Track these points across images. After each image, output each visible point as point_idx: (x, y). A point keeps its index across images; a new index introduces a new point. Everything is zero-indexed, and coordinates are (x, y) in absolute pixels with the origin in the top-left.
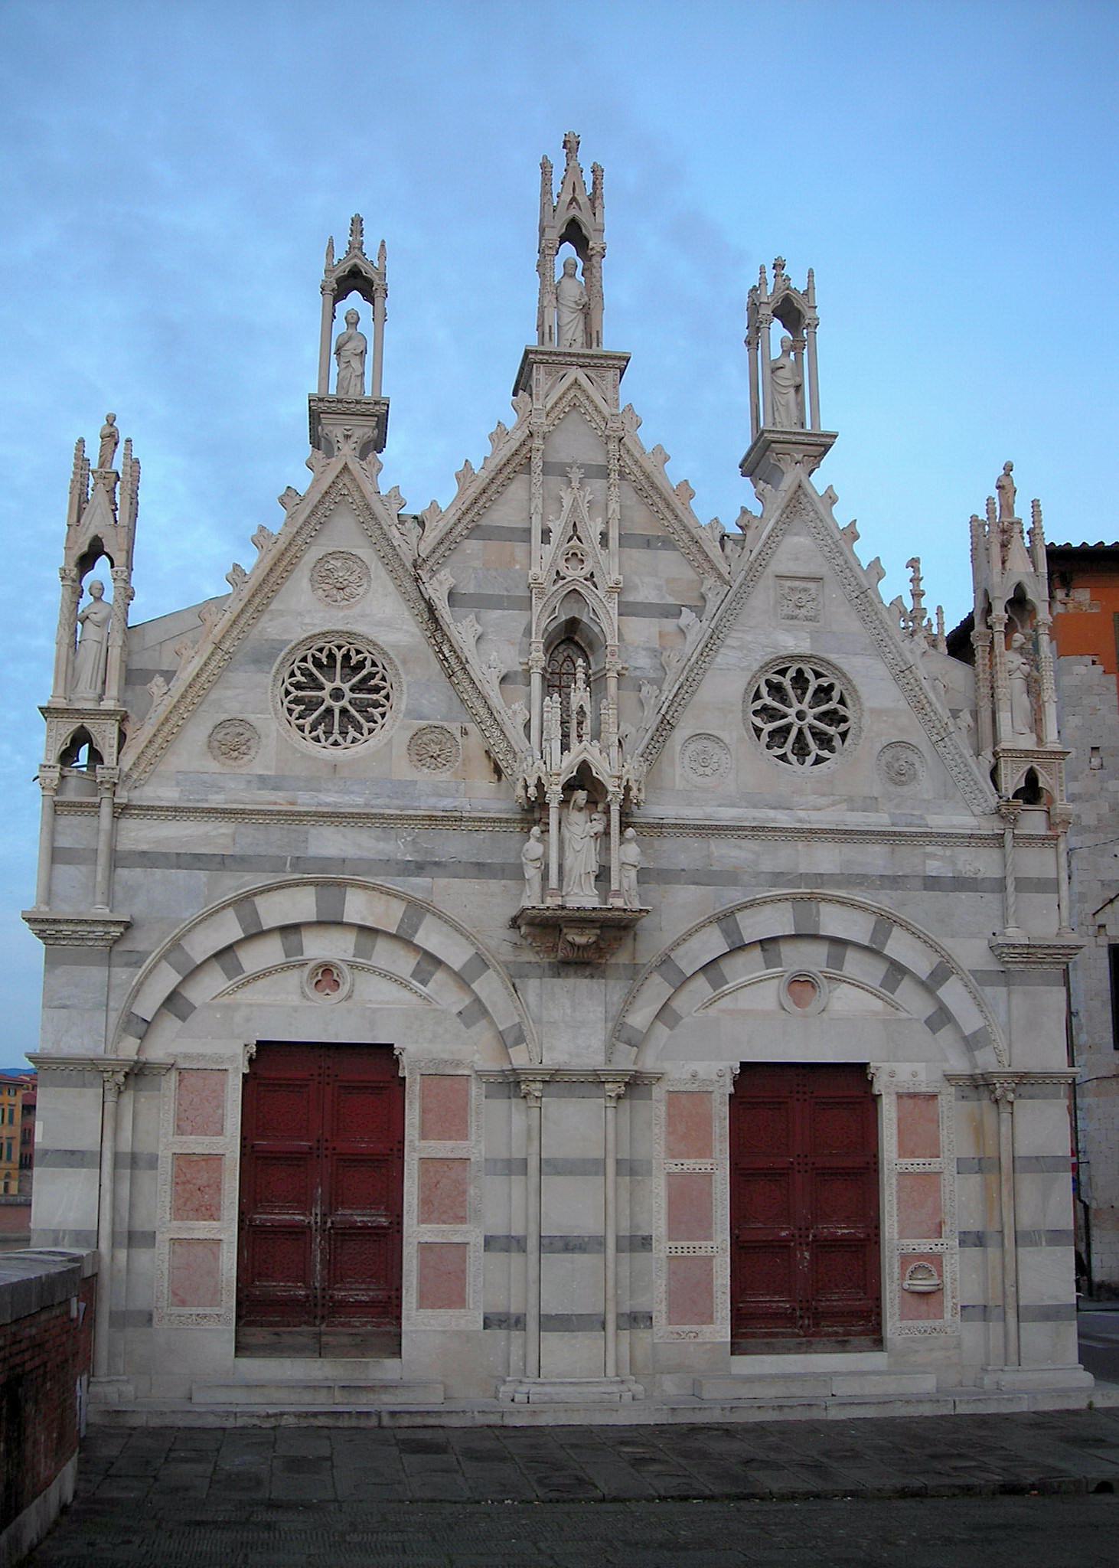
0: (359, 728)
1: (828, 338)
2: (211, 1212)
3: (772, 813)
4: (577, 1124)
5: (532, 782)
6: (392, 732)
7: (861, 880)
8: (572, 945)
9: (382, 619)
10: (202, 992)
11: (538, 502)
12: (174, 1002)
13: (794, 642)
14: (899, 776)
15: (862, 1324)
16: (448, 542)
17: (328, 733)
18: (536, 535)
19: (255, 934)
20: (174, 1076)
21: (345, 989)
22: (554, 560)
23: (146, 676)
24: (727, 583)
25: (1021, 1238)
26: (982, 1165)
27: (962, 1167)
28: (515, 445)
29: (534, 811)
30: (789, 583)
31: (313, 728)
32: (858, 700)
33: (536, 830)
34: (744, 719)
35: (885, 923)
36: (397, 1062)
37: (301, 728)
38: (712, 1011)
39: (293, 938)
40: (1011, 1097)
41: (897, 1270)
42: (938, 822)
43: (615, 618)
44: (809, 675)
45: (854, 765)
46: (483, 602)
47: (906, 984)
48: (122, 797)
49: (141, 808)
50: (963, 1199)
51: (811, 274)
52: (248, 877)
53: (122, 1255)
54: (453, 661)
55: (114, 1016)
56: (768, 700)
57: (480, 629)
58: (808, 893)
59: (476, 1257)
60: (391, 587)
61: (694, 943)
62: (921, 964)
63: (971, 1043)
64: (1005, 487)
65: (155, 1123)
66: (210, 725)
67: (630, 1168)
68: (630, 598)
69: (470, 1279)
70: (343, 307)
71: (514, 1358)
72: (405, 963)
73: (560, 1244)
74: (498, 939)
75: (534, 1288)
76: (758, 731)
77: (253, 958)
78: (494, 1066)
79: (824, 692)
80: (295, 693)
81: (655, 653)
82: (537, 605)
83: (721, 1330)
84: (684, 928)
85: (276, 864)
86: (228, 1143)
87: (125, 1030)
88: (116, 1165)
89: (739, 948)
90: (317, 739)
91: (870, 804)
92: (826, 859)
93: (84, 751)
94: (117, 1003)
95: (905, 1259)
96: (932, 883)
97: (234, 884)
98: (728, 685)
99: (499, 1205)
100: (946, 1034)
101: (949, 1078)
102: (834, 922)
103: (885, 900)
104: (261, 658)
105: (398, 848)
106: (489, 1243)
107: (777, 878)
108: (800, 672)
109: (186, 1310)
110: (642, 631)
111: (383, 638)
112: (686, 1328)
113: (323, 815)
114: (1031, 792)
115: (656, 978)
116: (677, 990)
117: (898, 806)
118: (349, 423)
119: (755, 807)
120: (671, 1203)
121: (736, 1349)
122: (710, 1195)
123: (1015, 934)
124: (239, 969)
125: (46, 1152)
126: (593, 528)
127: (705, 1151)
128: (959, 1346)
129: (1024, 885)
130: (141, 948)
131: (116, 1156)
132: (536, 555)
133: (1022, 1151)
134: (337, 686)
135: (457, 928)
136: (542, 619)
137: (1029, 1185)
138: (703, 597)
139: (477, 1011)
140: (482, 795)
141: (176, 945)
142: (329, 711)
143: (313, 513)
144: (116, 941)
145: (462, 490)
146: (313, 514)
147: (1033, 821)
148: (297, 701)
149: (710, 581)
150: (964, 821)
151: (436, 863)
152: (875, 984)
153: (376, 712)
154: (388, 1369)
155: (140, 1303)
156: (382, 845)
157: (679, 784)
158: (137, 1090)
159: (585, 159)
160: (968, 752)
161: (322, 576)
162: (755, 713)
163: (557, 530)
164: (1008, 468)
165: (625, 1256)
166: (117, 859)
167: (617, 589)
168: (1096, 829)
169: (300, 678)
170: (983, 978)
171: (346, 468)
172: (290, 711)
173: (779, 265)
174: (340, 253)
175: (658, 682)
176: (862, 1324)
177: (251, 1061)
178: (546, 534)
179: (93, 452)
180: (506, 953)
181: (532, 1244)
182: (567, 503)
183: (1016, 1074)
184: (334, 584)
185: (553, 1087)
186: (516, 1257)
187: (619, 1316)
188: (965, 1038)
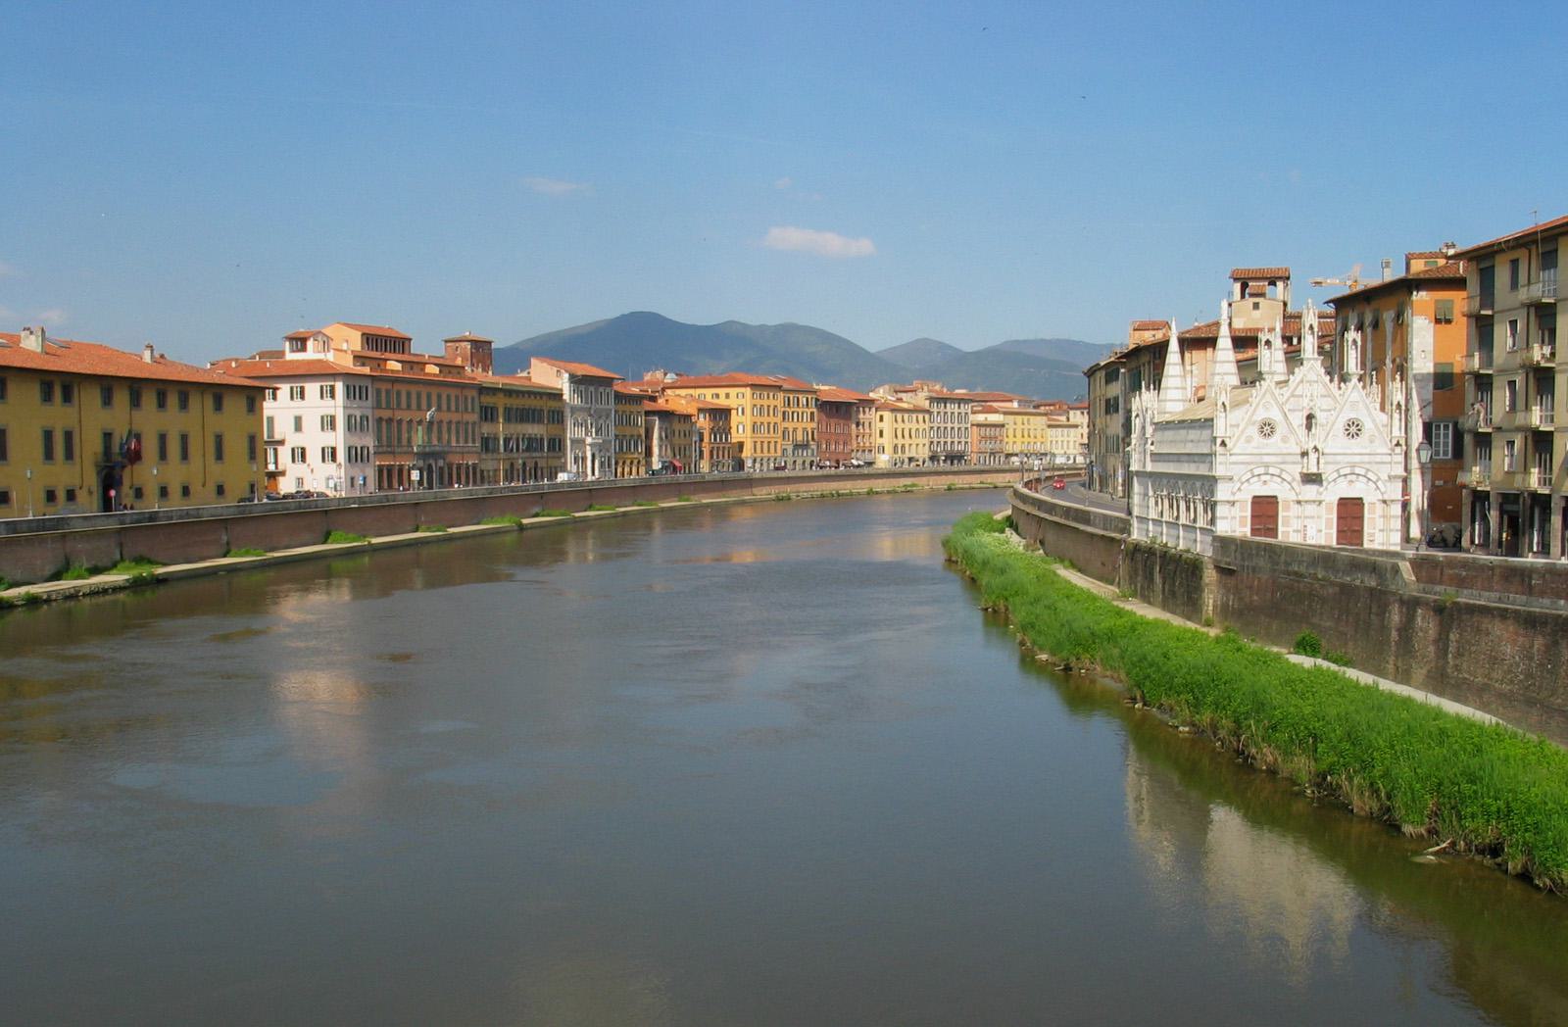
2: (1245, 526)
4: (1310, 509)
6: (1277, 437)
12: (1239, 489)
14: (1372, 442)
25: (1391, 530)
26: (1384, 517)
27: (1380, 517)
29: (1304, 454)
42: (1379, 451)
46: (1294, 410)
50: (1380, 523)
62: (1374, 478)
63: (1382, 494)
65: (1236, 511)
72: (1279, 480)
85: (1256, 463)
89: (1340, 476)
91: (1366, 448)
92: (1357, 459)
94: (1230, 489)
96: (1377, 463)
97: (1250, 467)
98: (1340, 425)
101: (1379, 500)
102: (1357, 471)
103: (1367, 466)
104: (1254, 424)
105: (1279, 459)
106: (1294, 531)
107: (1348, 463)
114: (1398, 444)
123: (1393, 474)
136: (1305, 414)
147: (1398, 450)
167: (1319, 408)
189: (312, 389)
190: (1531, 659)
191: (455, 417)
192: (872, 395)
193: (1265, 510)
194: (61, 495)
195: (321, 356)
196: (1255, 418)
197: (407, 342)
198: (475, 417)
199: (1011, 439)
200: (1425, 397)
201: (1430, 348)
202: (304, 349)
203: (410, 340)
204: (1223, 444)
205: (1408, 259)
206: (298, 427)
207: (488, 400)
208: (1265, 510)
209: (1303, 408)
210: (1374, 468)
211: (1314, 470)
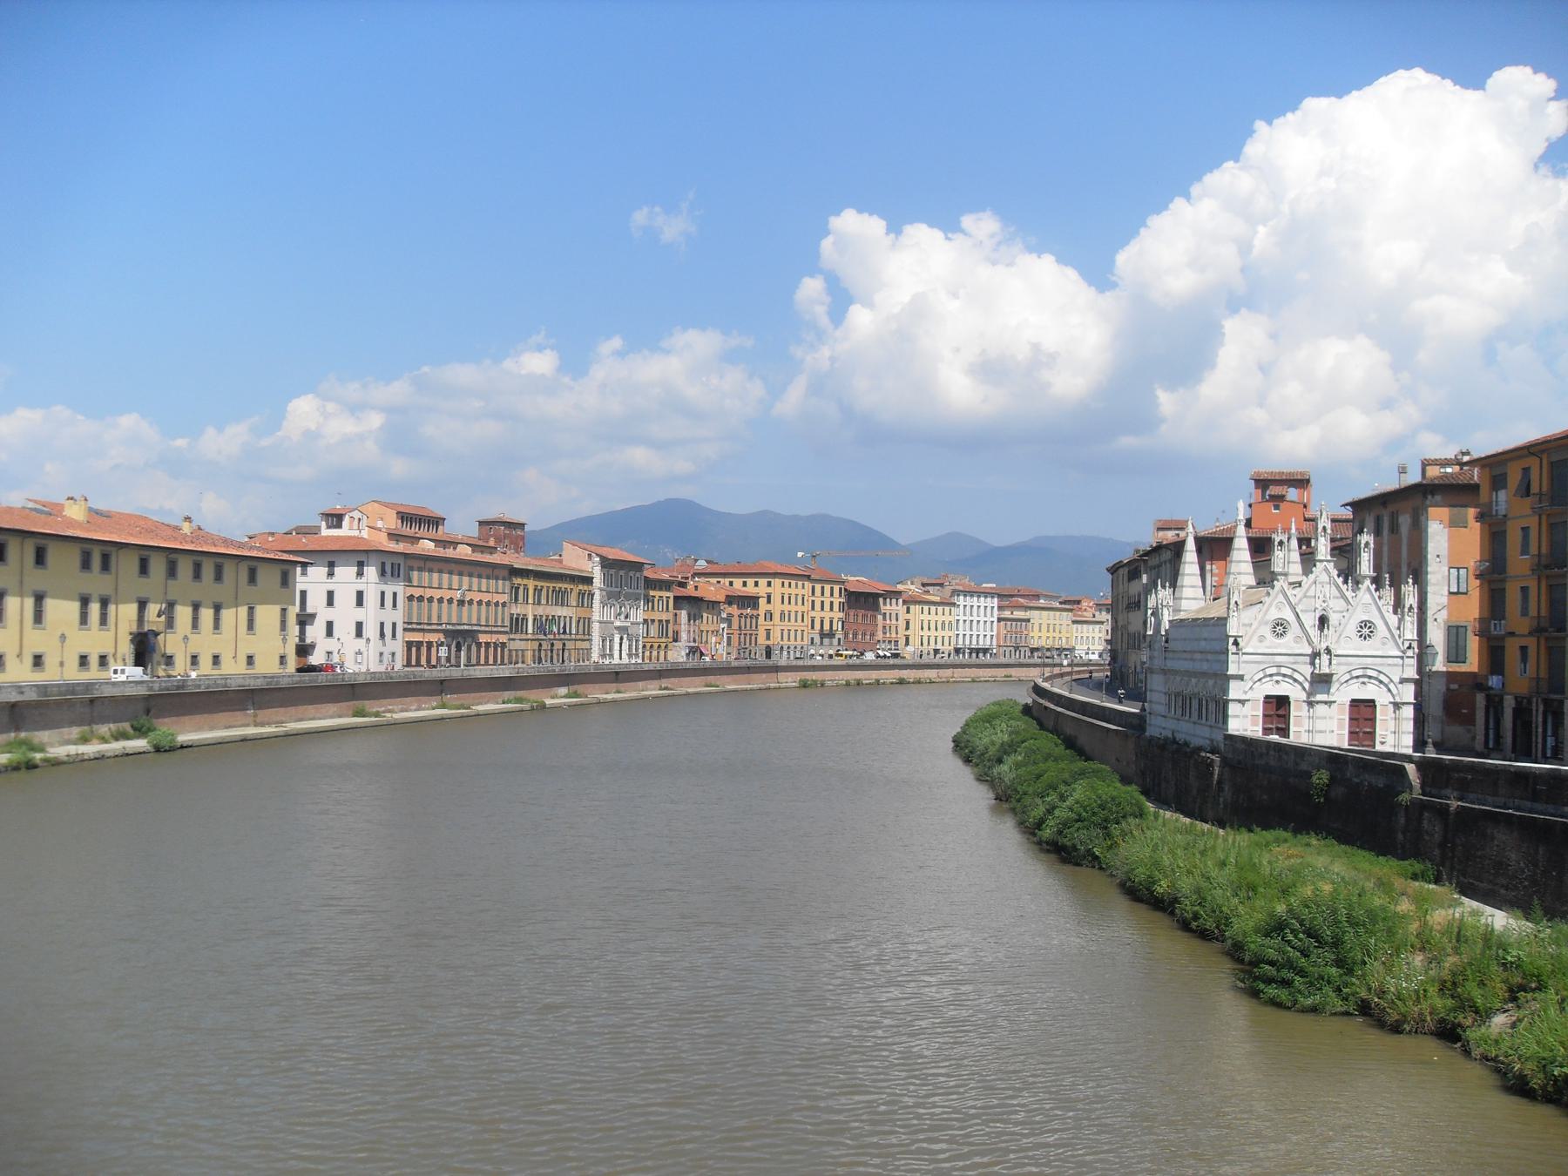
6: (1289, 637)
62: (1386, 680)
86: (1260, 713)
147: (1410, 653)
190: (1536, 865)
192: (900, 587)
193: (1278, 707)
194: (94, 661)
195: (356, 533)
198: (505, 598)
199: (1036, 634)
201: (1444, 552)
202: (339, 526)
204: (1236, 643)
205: (1425, 464)
206: (330, 602)
208: (1278, 707)
211: (1326, 670)
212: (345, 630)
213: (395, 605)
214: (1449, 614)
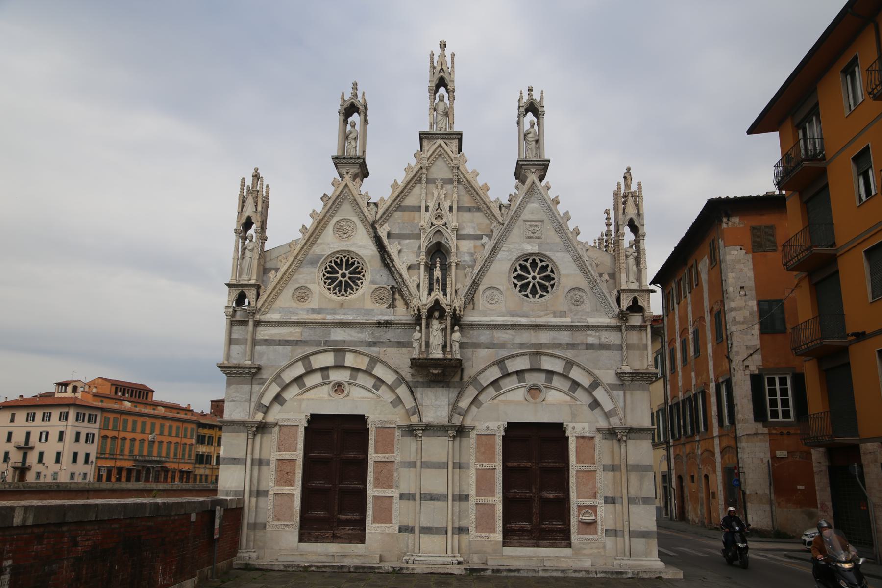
0: (352, 289)
1: (547, 120)
2: (291, 483)
3: (519, 319)
4: (437, 448)
5: (416, 309)
7: (559, 346)
8: (433, 374)
9: (362, 245)
10: (287, 395)
11: (424, 195)
12: (278, 399)
13: (530, 248)
15: (562, 537)
16: (387, 214)
17: (340, 291)
18: (423, 209)
19: (310, 372)
20: (277, 428)
21: (346, 392)
22: (430, 218)
23: (270, 269)
24: (503, 224)
25: (631, 501)
26: (614, 468)
27: (605, 468)
28: (415, 172)
30: (528, 224)
31: (334, 289)
32: (558, 271)
33: (418, 328)
34: (509, 280)
35: (570, 364)
36: (366, 422)
37: (329, 289)
38: (495, 401)
39: (326, 373)
40: (625, 438)
41: (576, 513)
42: (592, 321)
43: (455, 241)
44: (538, 261)
45: (557, 298)
46: (401, 237)
47: (579, 390)
48: (258, 317)
49: (265, 322)
50: (604, 482)
51: (542, 93)
52: (306, 348)
53: (254, 500)
54: (388, 260)
55: (253, 404)
56: (520, 272)
57: (400, 248)
58: (537, 353)
59: (396, 503)
60: (365, 232)
61: (487, 373)
62: (586, 381)
63: (607, 415)
64: (627, 177)
65: (269, 447)
66: (293, 289)
67: (460, 466)
68: (462, 232)
69: (394, 511)
70: (350, 119)
71: (410, 545)
72: (369, 382)
73: (429, 497)
74: (407, 372)
75: (418, 515)
76: (515, 285)
77: (309, 381)
78: (405, 423)
79: (544, 268)
80: (327, 275)
81: (472, 255)
82: (423, 237)
83: (499, 536)
84: (482, 367)
85: (318, 343)
86: (298, 455)
87: (258, 410)
88: (252, 464)
90: (335, 293)
91: (563, 314)
92: (544, 337)
93: (246, 302)
94: (254, 399)
95: (580, 507)
96: (590, 347)
97: (301, 351)
99: (406, 481)
100: (597, 411)
101: (599, 430)
102: (547, 364)
103: (570, 354)
104: (313, 262)
105: (366, 335)
106: (402, 496)
107: (522, 346)
108: (534, 260)
109: (279, 523)
110: (466, 246)
111: (361, 252)
112: (484, 534)
113: (336, 323)
115: (471, 388)
116: (480, 392)
117: (575, 315)
118: (353, 165)
119: (513, 316)
120: (478, 481)
121: (505, 544)
122: (494, 477)
123: (627, 369)
124: (304, 385)
125: (224, 459)
126: (446, 205)
127: (492, 459)
128: (604, 547)
129: (629, 347)
130: (264, 377)
131: (252, 460)
132: (423, 216)
133: (630, 462)
134: (343, 273)
135: (390, 367)
136: (424, 243)
137: (633, 477)
138: (492, 231)
139: (398, 401)
140: (401, 314)
141: (278, 376)
142: (341, 282)
143: (333, 203)
144: (254, 375)
145: (393, 192)
146: (333, 204)
147: (636, 320)
148: (328, 278)
149: (495, 224)
150: (606, 320)
151: (382, 342)
152: (566, 389)
153: (359, 282)
154: (358, 548)
155: (261, 520)
156: (360, 335)
157: (481, 308)
158: (263, 433)
159: (448, 52)
160: (606, 291)
161: (338, 228)
162: (514, 278)
163: (431, 205)
164: (629, 169)
165: (457, 503)
166: (255, 342)
167: (456, 230)
168: (743, 323)
169: (329, 269)
170: (613, 387)
171: (346, 185)
172: (325, 283)
173: (530, 90)
174: (347, 97)
175: (472, 267)
176: (562, 537)
177: (308, 422)
178: (427, 209)
179: (249, 182)
180: (408, 378)
181: (418, 497)
182: (436, 195)
183: (626, 429)
184: (343, 231)
185: (427, 432)
186: (411, 502)
187: (453, 528)
188: (605, 413)
189: (56, 414)
191: (185, 441)
196: (317, 250)
197: (150, 394)
198: (194, 441)
200: (750, 344)
201: (751, 283)
202: (66, 392)
203: (153, 391)
207: (202, 431)
209: (422, 229)
210: (583, 357)
212: (49, 458)
213: (92, 442)
214: (764, 359)
